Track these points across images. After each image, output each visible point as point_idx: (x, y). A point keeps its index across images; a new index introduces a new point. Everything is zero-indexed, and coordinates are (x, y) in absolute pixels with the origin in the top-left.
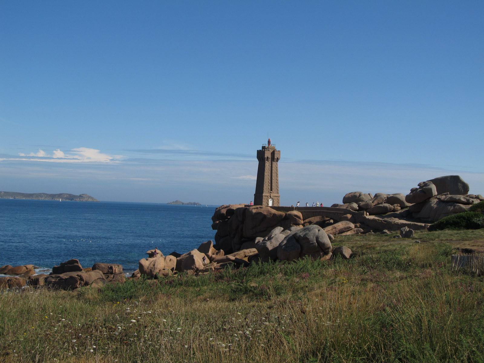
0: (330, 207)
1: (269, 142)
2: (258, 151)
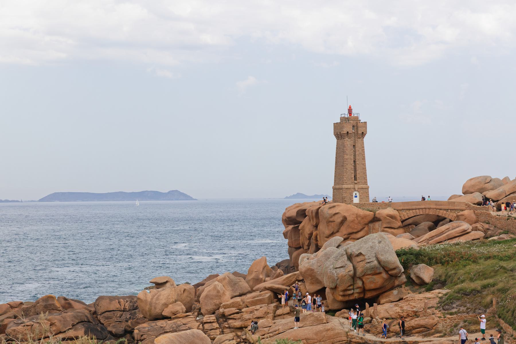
0: (446, 200)
1: (350, 111)
2: (334, 124)
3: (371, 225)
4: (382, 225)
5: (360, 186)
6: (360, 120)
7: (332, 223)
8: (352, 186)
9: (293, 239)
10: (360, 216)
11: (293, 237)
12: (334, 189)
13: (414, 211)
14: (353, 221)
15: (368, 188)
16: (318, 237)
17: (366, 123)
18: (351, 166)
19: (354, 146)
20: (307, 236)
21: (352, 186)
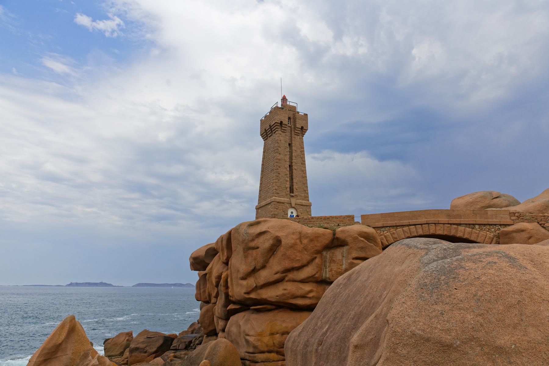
3: (327, 254)
4: (349, 253)
5: (299, 201)
6: (298, 113)
7: (254, 252)
8: (286, 200)
9: (202, 290)
10: (306, 236)
11: (202, 287)
12: (257, 209)
13: (406, 229)
14: (292, 246)
15: (309, 206)
16: (229, 280)
17: (306, 115)
18: (284, 170)
19: (289, 144)
20: (214, 281)
21: (286, 200)
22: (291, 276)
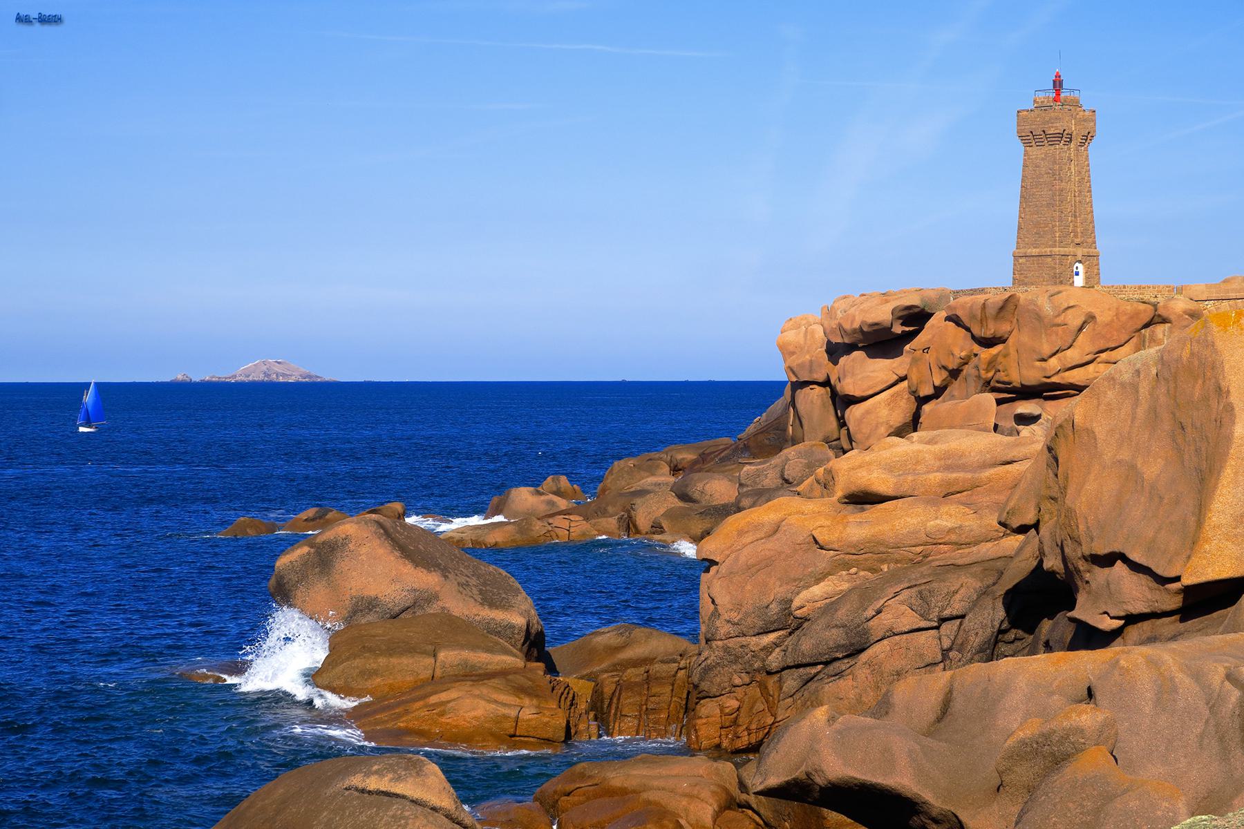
7: (1060, 329)
13: (1231, 302)
22: (1103, 356)
